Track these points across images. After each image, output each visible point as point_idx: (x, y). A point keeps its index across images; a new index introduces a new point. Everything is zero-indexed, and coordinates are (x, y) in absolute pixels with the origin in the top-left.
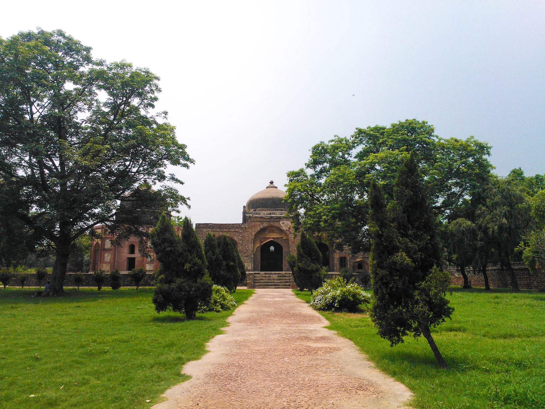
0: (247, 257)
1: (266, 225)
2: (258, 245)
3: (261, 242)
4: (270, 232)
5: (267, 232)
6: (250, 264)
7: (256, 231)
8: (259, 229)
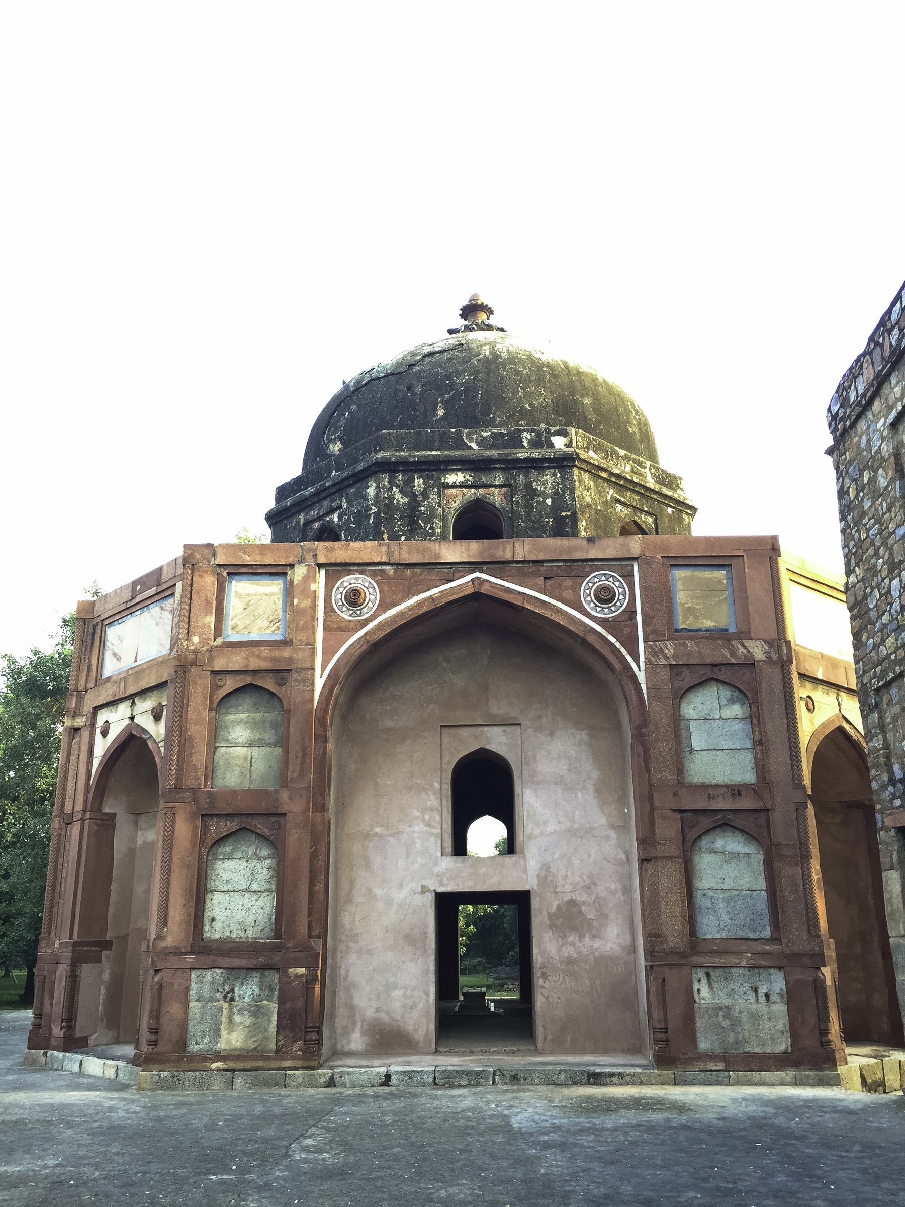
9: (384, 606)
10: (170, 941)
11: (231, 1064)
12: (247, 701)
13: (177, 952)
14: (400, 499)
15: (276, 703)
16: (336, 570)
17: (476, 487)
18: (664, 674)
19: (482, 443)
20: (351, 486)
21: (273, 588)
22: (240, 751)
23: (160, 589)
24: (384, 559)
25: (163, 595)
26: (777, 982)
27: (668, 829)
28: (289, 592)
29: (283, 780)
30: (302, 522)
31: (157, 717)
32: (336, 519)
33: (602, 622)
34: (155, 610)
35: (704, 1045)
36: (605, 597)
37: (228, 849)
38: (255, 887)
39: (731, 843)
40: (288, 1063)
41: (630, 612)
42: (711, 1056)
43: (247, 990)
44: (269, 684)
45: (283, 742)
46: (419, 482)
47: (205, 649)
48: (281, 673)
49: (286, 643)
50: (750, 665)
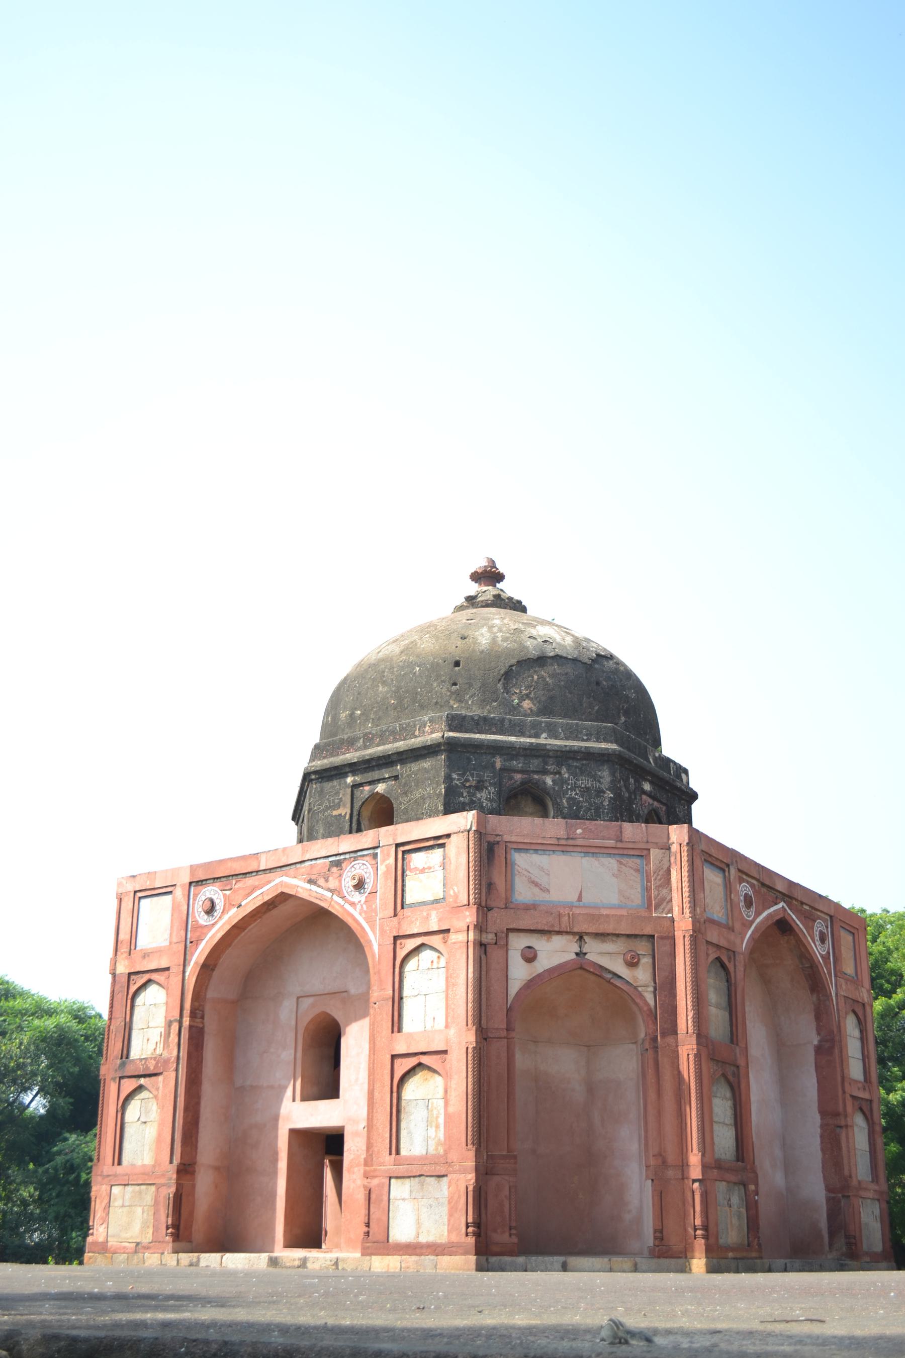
9: (758, 914)
11: (738, 1255)
15: (723, 974)
17: (654, 798)
18: (843, 999)
19: (655, 759)
20: (574, 759)
23: (619, 845)
24: (756, 876)
25: (621, 852)
28: (728, 887)
30: (498, 765)
31: (632, 964)
33: (822, 956)
34: (612, 862)
35: (865, 1248)
37: (714, 1088)
38: (727, 1122)
40: (754, 1254)
41: (828, 953)
42: (867, 1254)
46: (632, 781)
47: (702, 920)
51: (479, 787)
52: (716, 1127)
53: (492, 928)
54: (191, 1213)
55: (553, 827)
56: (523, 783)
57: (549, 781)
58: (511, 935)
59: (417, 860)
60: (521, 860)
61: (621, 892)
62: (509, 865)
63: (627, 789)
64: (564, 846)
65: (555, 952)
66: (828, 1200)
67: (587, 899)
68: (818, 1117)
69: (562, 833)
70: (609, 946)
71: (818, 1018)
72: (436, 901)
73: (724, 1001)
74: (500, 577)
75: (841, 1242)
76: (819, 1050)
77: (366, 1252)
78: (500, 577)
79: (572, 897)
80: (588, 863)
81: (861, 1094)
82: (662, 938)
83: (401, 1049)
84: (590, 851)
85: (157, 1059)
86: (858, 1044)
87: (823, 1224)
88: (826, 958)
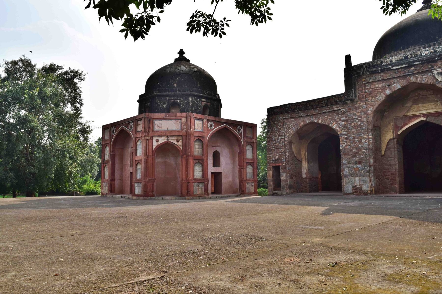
0: (360, 162)
1: (399, 86)
2: (389, 135)
3: (397, 128)
4: (416, 102)
5: (409, 104)
6: (367, 179)
7: (376, 104)
8: (381, 97)
9: (215, 128)
10: (191, 178)
12: (197, 141)
13: (192, 180)
14: (196, 102)
16: (209, 121)
21: (200, 122)
22: (197, 149)
26: (253, 184)
27: (245, 164)
28: (203, 124)
29: (203, 154)
31: (178, 141)
32: (179, 101)
34: (174, 121)
35: (247, 192)
36: (239, 130)
39: (250, 166)
43: (200, 185)
44: (201, 139)
45: (203, 148)
46: (198, 99)
48: (203, 137)
49: (203, 132)
50: (253, 143)
51: (164, 104)
52: (195, 172)
53: (149, 136)
54: (114, 188)
55: (163, 115)
56: (173, 102)
57: (179, 101)
58: (154, 137)
59: (139, 122)
60: (156, 122)
61: (176, 127)
62: (153, 123)
63: (197, 101)
64: (164, 118)
65: (162, 140)
66: (240, 184)
67: (170, 129)
68: (238, 167)
69: (164, 116)
70: (173, 138)
71: (239, 147)
72: (141, 131)
73: (201, 147)
74: (184, 53)
75: (241, 191)
76: (239, 153)
77: (132, 196)
78: (184, 53)
79: (166, 129)
80: (170, 122)
81: (250, 161)
82: (184, 136)
83: (136, 159)
84: (170, 119)
85: (108, 160)
86: (251, 151)
87: (238, 187)
88: (241, 135)
